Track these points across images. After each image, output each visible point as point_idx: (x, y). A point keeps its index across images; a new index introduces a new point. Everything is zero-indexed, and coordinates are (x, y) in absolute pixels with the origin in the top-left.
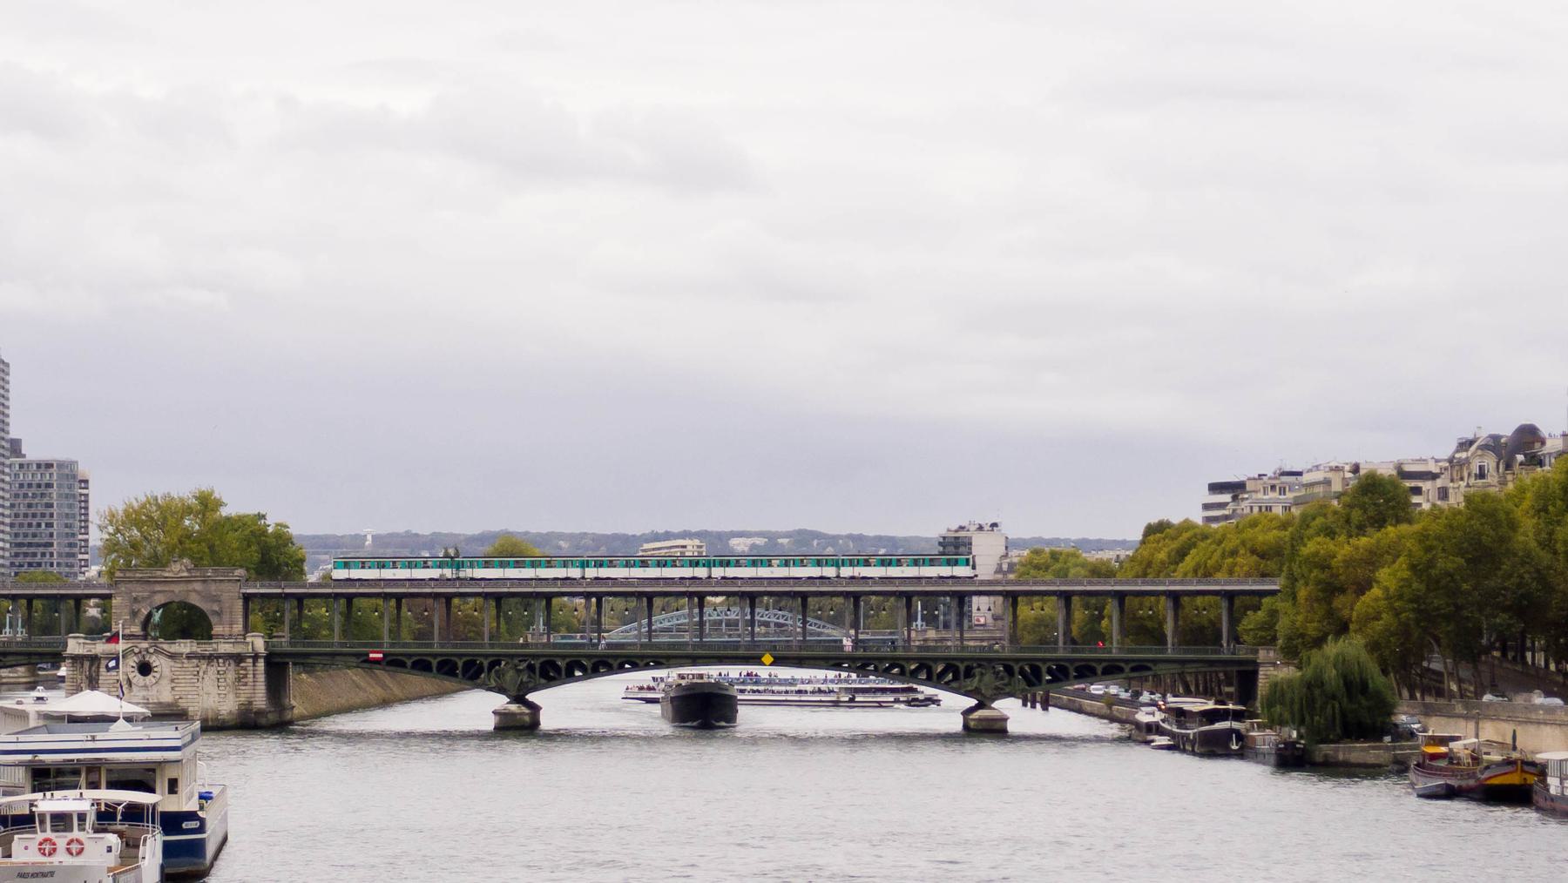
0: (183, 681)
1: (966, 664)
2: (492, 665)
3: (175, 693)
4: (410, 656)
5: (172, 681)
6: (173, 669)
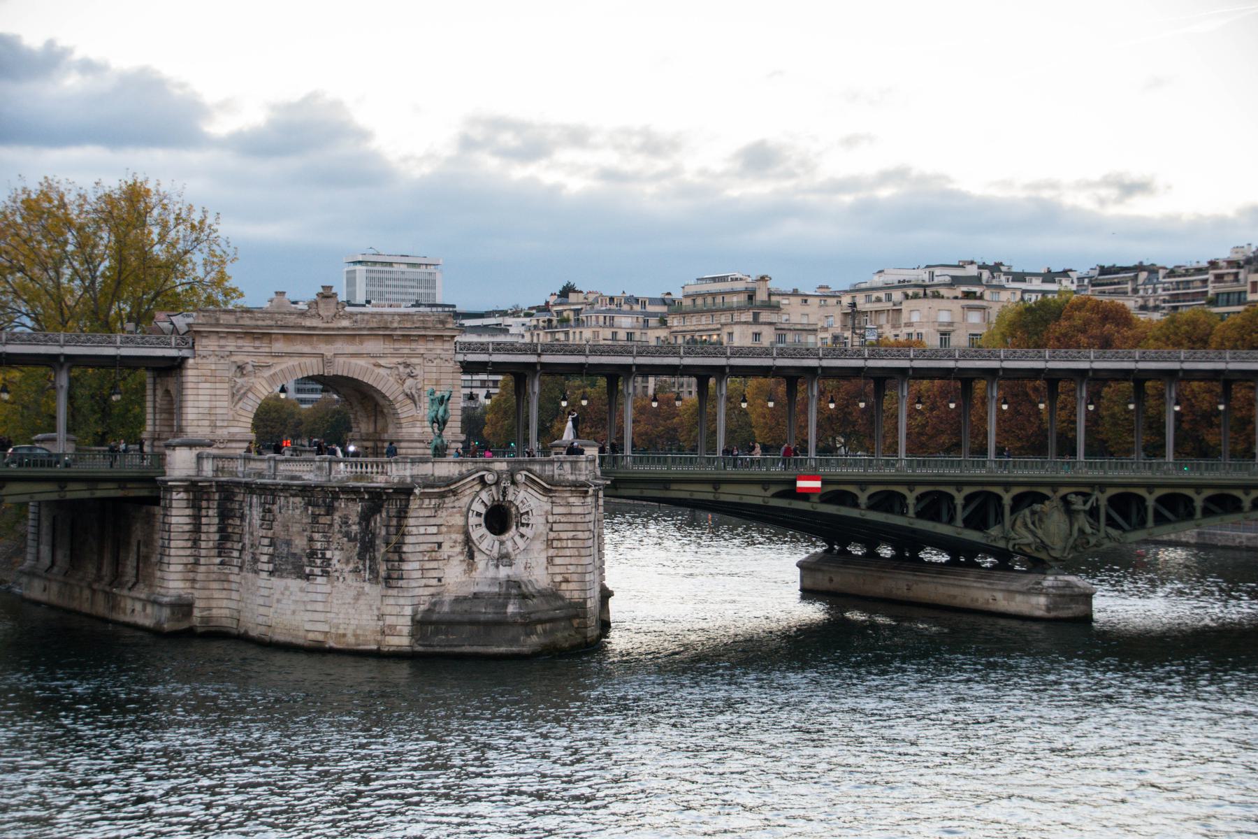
0: (570, 544)
2: (1019, 502)
3: (557, 570)
4: (863, 484)
5: (549, 543)
6: (551, 519)
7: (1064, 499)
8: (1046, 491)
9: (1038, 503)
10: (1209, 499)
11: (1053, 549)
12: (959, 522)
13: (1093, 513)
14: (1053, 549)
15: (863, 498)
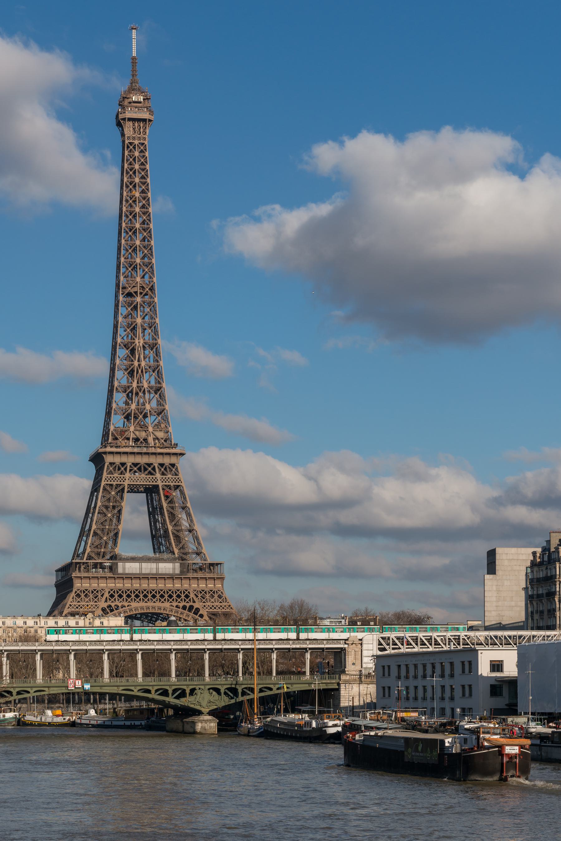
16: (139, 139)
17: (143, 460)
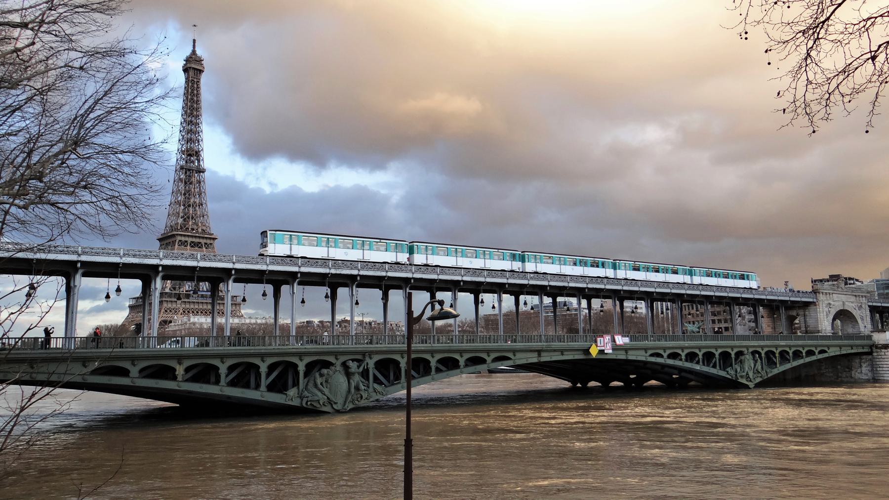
1: (736, 350)
2: (310, 367)
7: (344, 364)
8: (331, 359)
9: (326, 368)
10: (440, 361)
11: (336, 403)
12: (263, 387)
13: (365, 374)
14: (336, 403)
15: (180, 370)
16: (197, 79)
17: (197, 240)
